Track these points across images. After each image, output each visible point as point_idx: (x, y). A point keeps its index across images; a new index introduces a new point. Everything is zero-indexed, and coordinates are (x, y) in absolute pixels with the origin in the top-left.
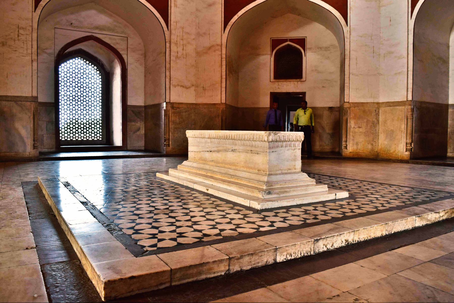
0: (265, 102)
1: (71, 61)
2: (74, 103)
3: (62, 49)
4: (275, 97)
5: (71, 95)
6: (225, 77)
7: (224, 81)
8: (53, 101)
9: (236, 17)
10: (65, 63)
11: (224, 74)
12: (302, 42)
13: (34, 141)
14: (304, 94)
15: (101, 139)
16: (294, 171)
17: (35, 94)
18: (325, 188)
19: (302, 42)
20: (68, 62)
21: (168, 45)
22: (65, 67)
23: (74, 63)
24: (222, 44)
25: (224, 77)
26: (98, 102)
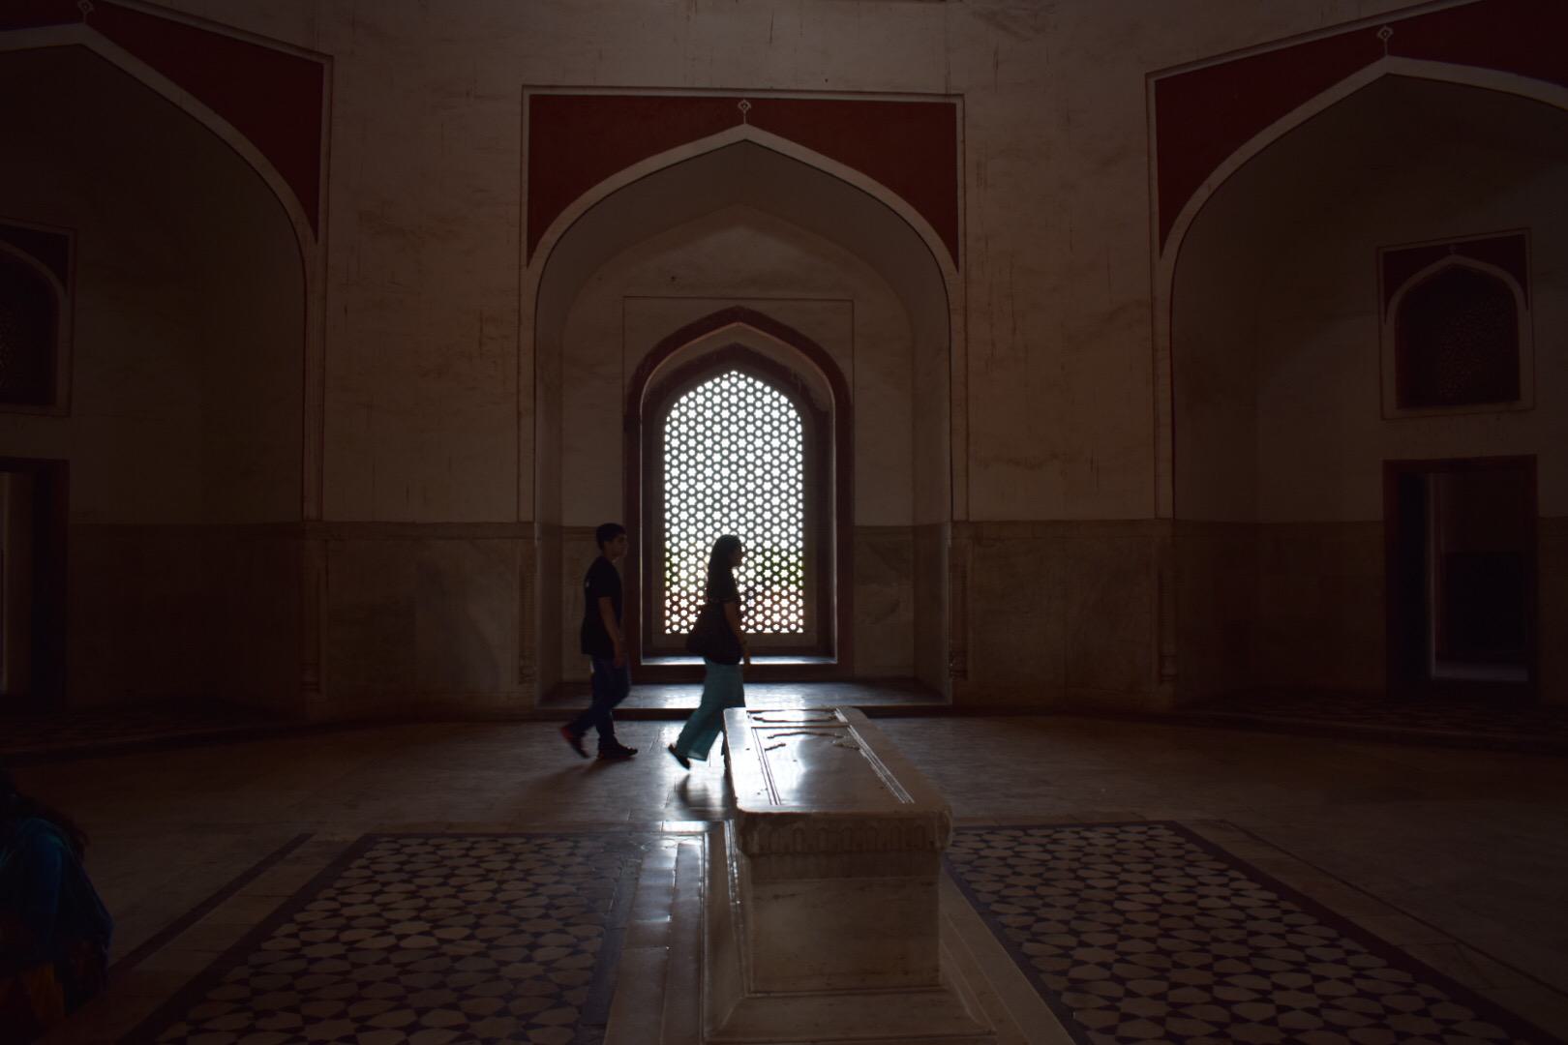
1: (709, 385)
2: (717, 515)
4: (1405, 481)
5: (709, 492)
6: (1168, 420)
7: (1166, 432)
9: (1202, 194)
10: (692, 394)
11: (1165, 407)
12: (1511, 251)
14: (1525, 466)
17: (526, 515)
19: (1511, 251)
20: (700, 389)
21: (957, 320)
22: (692, 404)
23: (717, 390)
25: (1166, 420)
26: (793, 510)
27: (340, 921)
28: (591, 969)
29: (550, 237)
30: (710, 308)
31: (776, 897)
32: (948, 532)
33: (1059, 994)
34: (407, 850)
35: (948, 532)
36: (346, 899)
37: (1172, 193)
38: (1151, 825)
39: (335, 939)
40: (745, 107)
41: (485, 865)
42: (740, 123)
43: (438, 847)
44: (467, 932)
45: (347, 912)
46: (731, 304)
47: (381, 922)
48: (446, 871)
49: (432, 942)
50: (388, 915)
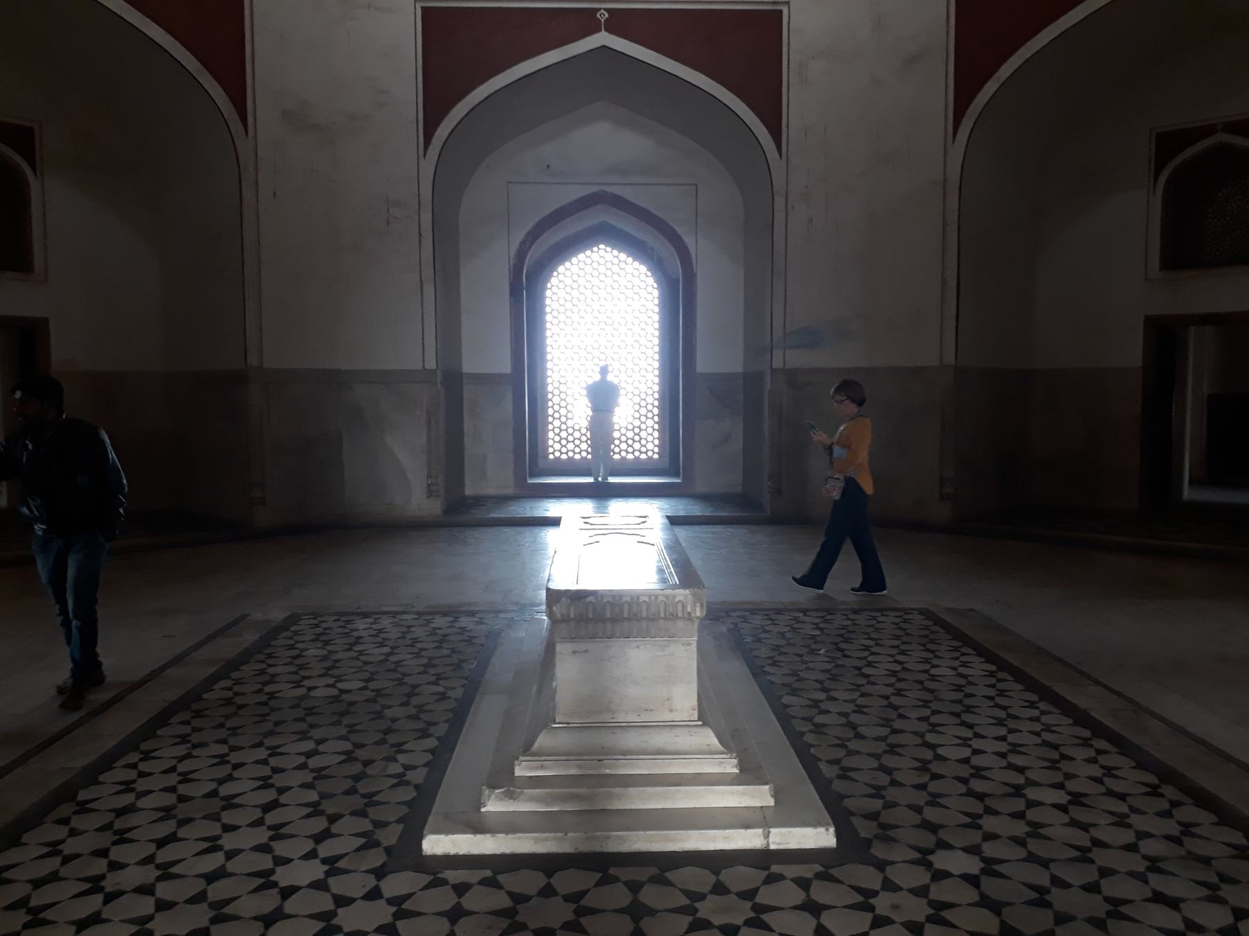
0: (1129, 352)
3: (527, 235)
8: (506, 367)
9: (991, 87)
13: (429, 476)
15: (656, 456)
16: (667, 716)
17: (431, 364)
18: (759, 797)
21: (779, 202)
24: (945, 179)
27: (266, 678)
28: (451, 710)
29: (442, 132)
30: (576, 192)
31: (574, 652)
32: (768, 379)
33: (803, 734)
34: (324, 625)
35: (768, 379)
36: (270, 661)
37: (966, 84)
38: (907, 611)
39: (260, 691)
40: (603, 16)
41: (382, 635)
42: (598, 30)
43: (348, 622)
44: (362, 684)
45: (271, 670)
46: (594, 189)
47: (297, 678)
48: (351, 640)
49: (335, 692)
50: (302, 673)
